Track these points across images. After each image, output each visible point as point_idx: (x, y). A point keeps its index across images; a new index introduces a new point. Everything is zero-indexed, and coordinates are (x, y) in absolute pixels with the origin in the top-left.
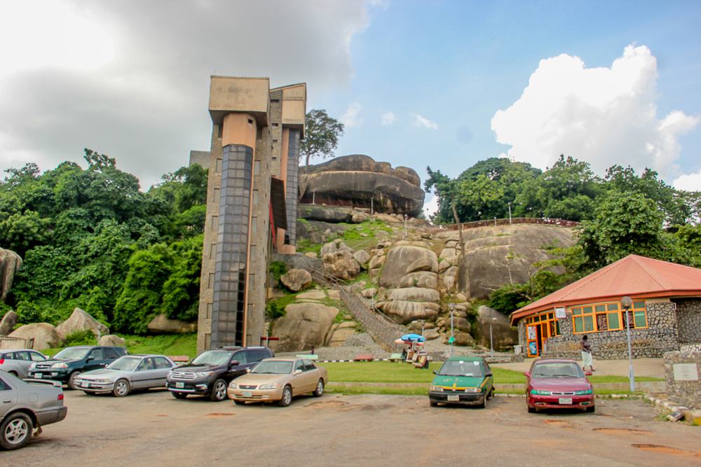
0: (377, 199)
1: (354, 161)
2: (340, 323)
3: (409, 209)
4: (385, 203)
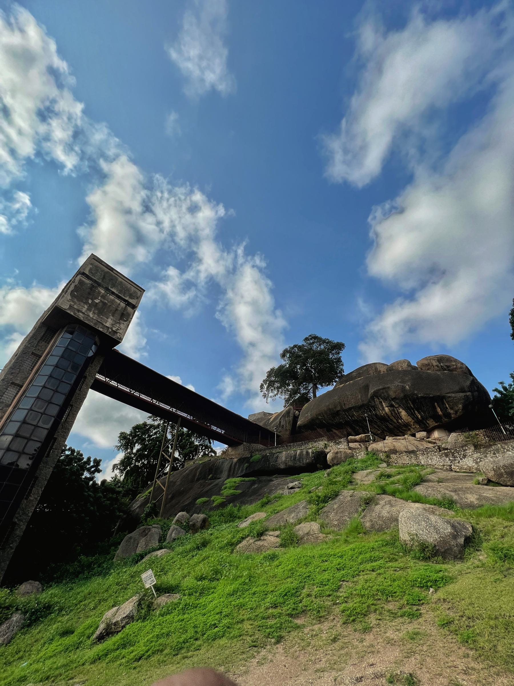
3: (448, 415)
4: (398, 416)
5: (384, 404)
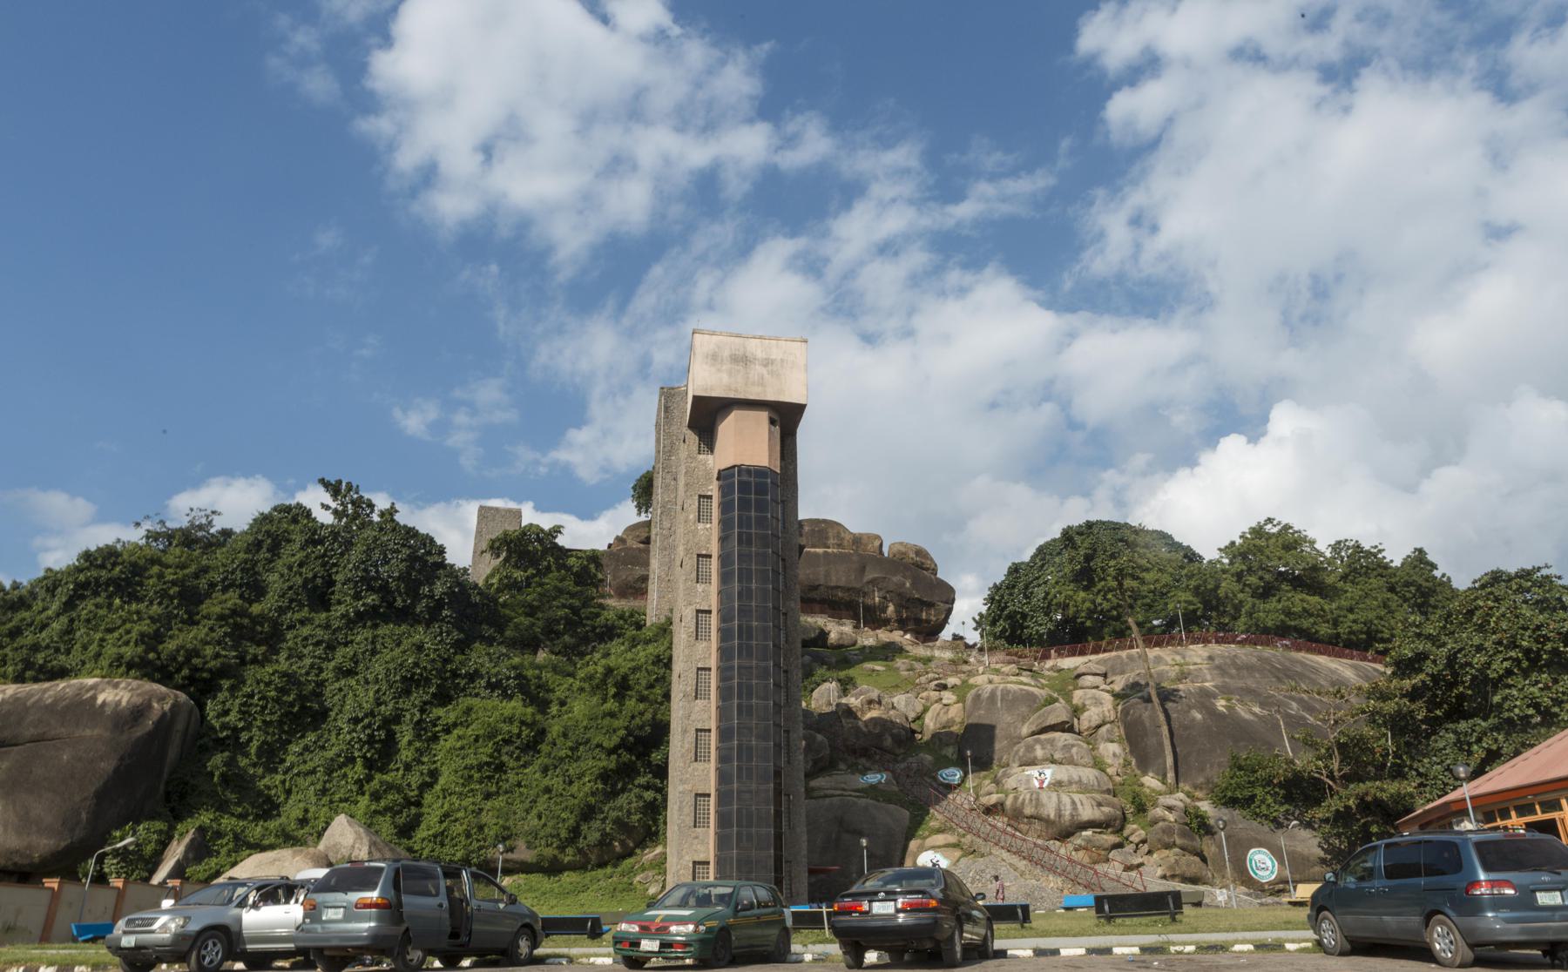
0: (869, 602)
1: (813, 530)
2: (925, 838)
4: (884, 610)
5: (876, 594)
